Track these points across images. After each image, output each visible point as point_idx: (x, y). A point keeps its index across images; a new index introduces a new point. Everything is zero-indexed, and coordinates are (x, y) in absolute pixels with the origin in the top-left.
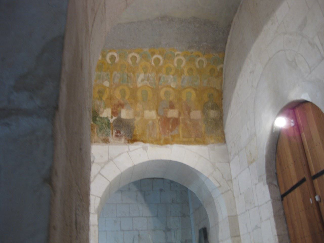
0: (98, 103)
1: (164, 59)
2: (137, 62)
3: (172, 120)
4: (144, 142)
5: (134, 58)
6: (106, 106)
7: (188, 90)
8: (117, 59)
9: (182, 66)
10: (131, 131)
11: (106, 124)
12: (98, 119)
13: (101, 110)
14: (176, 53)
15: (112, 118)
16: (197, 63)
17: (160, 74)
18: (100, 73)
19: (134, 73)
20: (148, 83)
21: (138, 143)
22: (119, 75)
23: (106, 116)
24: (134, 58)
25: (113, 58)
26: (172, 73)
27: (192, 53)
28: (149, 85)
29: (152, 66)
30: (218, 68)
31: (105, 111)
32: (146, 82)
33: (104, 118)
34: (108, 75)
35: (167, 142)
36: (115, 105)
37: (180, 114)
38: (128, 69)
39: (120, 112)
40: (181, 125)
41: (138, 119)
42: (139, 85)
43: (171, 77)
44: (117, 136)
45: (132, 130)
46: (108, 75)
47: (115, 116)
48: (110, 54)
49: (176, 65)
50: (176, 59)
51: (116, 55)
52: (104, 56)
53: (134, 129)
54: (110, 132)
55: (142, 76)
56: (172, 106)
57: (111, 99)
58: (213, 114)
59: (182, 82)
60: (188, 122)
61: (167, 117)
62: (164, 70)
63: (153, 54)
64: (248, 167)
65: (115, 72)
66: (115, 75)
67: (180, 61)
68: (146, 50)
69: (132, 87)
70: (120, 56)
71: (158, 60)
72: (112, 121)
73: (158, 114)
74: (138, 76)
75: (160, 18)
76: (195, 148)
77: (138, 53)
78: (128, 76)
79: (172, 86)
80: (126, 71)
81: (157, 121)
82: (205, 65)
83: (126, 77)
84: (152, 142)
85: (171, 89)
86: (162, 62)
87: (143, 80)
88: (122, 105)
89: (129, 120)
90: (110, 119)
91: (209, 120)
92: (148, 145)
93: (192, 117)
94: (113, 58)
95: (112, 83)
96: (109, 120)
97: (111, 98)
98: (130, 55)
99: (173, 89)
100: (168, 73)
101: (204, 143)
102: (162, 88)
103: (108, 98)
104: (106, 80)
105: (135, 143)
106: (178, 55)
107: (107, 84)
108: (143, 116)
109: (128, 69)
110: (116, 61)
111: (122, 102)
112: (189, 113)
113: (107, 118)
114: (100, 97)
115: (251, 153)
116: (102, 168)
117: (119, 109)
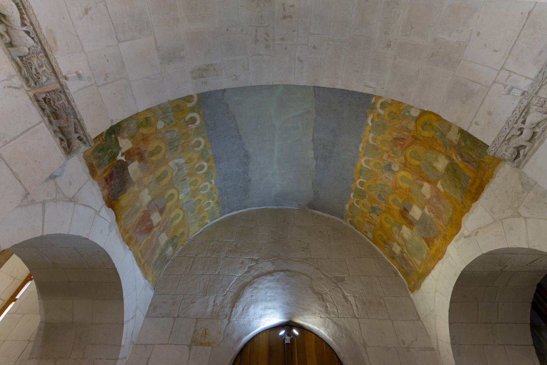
0: (132, 125)
2: (196, 149)
4: (117, 220)
5: (199, 144)
6: (132, 137)
7: (181, 213)
8: (193, 126)
9: (202, 192)
10: (119, 192)
11: (111, 153)
12: (113, 136)
13: (125, 135)
14: (213, 181)
15: (123, 154)
16: (207, 202)
17: (188, 178)
19: (182, 151)
21: (113, 212)
22: (175, 136)
23: (121, 145)
24: (199, 144)
27: (215, 193)
28: (174, 173)
29: (195, 165)
31: (126, 139)
33: (118, 145)
35: (128, 241)
36: (139, 148)
37: (158, 224)
39: (133, 161)
40: (150, 237)
41: (136, 188)
42: (171, 164)
43: (189, 189)
44: (106, 180)
45: (121, 192)
46: (172, 122)
47: (125, 158)
49: (201, 187)
50: (207, 183)
51: (198, 122)
52: (192, 110)
53: (123, 193)
54: (105, 165)
55: (181, 161)
56: (161, 212)
57: (143, 139)
59: (187, 202)
62: (194, 179)
63: (208, 161)
64: (190, 347)
65: (176, 129)
66: (175, 131)
67: (206, 187)
68: (210, 152)
69: (167, 157)
70: (198, 127)
71: (202, 167)
72: (120, 157)
73: (149, 205)
74: (180, 158)
76: (138, 272)
77: (205, 146)
79: (180, 196)
80: (182, 141)
82: (206, 209)
84: (120, 227)
85: (177, 196)
86: (201, 172)
87: (177, 164)
88: (141, 158)
90: (120, 154)
92: (116, 226)
93: (159, 238)
94: (193, 120)
95: (163, 132)
96: (117, 154)
97: (145, 139)
98: (200, 139)
99: (178, 198)
100: (191, 184)
101: (146, 276)
102: (175, 188)
103: (143, 135)
104: (165, 122)
105: (111, 209)
106: (211, 183)
107: (160, 125)
108: (140, 192)
110: (190, 126)
111: (146, 155)
112: (162, 232)
113: (120, 148)
114: (141, 123)
115: (206, 332)
116: (55, 200)
117: (137, 157)
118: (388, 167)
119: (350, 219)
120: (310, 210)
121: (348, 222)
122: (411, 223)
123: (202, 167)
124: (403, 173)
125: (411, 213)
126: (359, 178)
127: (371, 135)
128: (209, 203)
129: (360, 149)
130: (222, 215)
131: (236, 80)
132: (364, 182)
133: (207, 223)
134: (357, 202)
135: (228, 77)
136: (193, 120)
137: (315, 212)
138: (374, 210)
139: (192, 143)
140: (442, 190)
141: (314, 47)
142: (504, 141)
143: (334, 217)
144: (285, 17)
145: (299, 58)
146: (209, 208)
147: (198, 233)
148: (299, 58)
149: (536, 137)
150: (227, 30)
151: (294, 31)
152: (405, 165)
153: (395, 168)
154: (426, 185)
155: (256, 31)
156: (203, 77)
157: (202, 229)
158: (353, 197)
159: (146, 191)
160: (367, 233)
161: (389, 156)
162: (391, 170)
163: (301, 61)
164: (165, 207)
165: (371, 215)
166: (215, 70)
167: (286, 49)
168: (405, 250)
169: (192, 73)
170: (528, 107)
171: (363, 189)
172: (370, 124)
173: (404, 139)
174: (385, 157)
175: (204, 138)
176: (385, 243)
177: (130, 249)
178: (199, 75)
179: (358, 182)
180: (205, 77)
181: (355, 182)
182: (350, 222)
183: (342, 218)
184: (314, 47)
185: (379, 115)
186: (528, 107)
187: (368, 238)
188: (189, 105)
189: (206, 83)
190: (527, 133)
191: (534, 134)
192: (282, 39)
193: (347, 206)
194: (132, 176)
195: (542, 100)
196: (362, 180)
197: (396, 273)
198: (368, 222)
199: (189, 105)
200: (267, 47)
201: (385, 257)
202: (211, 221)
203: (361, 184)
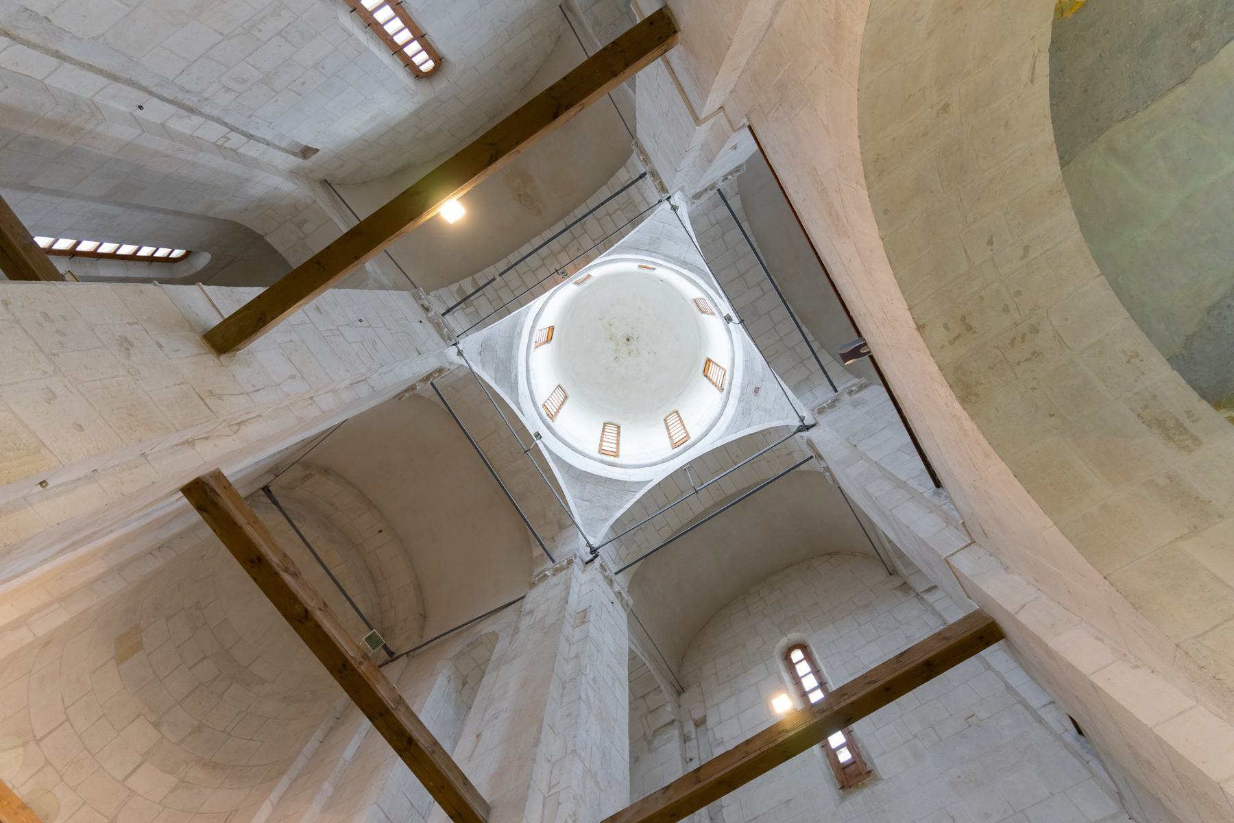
131: (1137, 355)
135: (1143, 373)
141: (990, 242)
144: (969, 328)
145: (1023, 258)
148: (1025, 256)
150: (1051, 415)
151: (982, 298)
155: (1019, 363)
156: (1179, 424)
163: (1027, 249)
166: (1146, 407)
167: (1018, 293)
169: (1189, 450)
178: (1181, 434)
180: (1177, 420)
184: (990, 242)
189: (1189, 413)
192: (1006, 309)
200: (1035, 330)
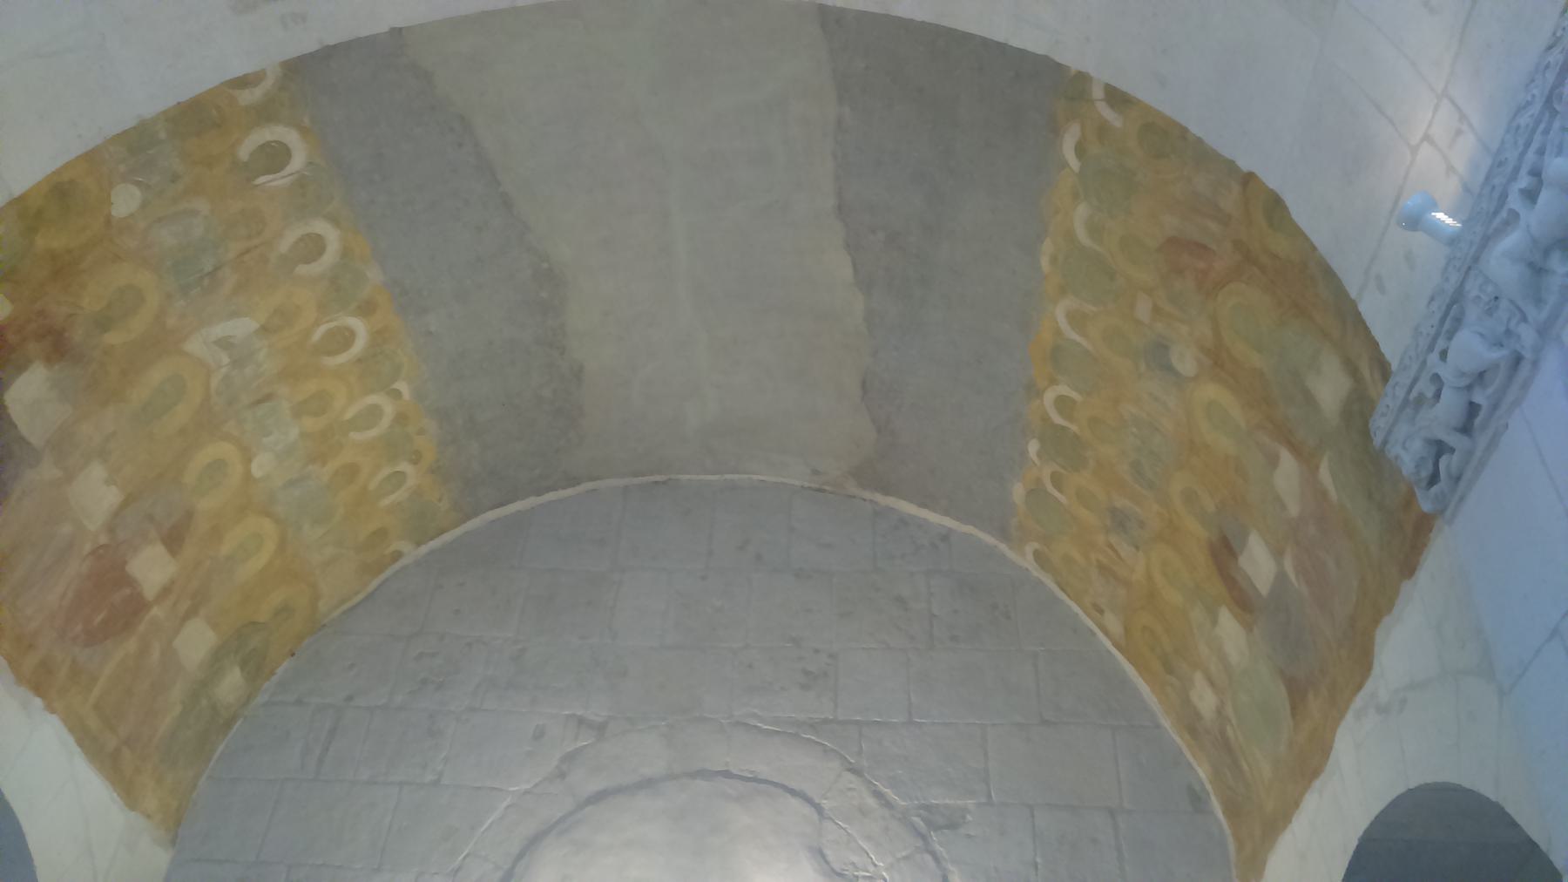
1: (359, 360)
2: (302, 269)
3: (127, 591)
5: (313, 247)
7: (268, 526)
9: (355, 436)
14: (402, 386)
16: (386, 471)
18: (163, 135)
20: (224, 370)
24: (313, 247)
25: (275, 156)
26: (309, 423)
27: (421, 432)
28: (215, 382)
30: (395, 546)
32: (226, 360)
34: (175, 178)
37: (166, 591)
38: (248, 251)
39: (21, 368)
40: (132, 645)
41: (47, 471)
42: (195, 346)
43: (294, 433)
46: (175, 178)
48: (291, 137)
49: (349, 415)
51: (298, 161)
52: (265, 113)
55: (241, 328)
58: (232, 682)
60: (156, 654)
61: (125, 563)
62: (312, 386)
65: (202, 205)
67: (374, 413)
68: (374, 275)
71: (347, 338)
74: (234, 314)
75: (545, 265)
76: (94, 787)
77: (346, 253)
78: (217, 269)
81: (88, 547)
82: (386, 502)
83: (208, 268)
86: (341, 359)
87: (225, 344)
88: (57, 346)
89: (22, 440)
91: (204, 702)
97: (64, 269)
98: (320, 227)
99: (248, 477)
100: (298, 412)
101: (128, 792)
106: (397, 394)
107: (125, 201)
109: (248, 251)
110: (261, 180)
118: (1158, 355)
119: (1036, 545)
120: (867, 495)
121: (1030, 557)
122: (1243, 601)
123: (344, 339)
124: (1211, 391)
125: (1243, 561)
126: (1053, 381)
127: (1082, 211)
128: (400, 477)
129: (1045, 263)
130: (468, 518)
132: (1074, 402)
133: (398, 556)
134: (1057, 480)
136: (275, 156)
137: (890, 501)
138: (1119, 521)
139: (285, 245)
140: (1333, 493)
142: (1406, 402)
143: (969, 529)
146: (399, 495)
147: (360, 597)
149: (1477, 421)
152: (1218, 361)
153: (1186, 361)
154: (1287, 461)
157: (375, 583)
158: (1039, 455)
159: (97, 471)
160: (1101, 612)
161: (1157, 311)
162: (1169, 369)
164: (189, 515)
165: (1113, 539)
168: (1229, 710)
170: (1458, 297)
171: (1074, 428)
172: (1074, 163)
173: (1205, 247)
174: (1143, 309)
175: (334, 220)
176: (1170, 670)
177: (51, 709)
179: (1049, 396)
181: (1039, 394)
182: (1037, 555)
183: (1003, 533)
185: (1103, 130)
186: (1458, 297)
187: (1106, 633)
188: (247, 97)
190: (1450, 405)
191: (1473, 409)
193: (1018, 492)
194: (24, 429)
195: (1490, 289)
196: (1063, 389)
197: (1197, 800)
198: (1102, 568)
199: (247, 97)
201: (1166, 723)
202: (418, 544)
203: (1063, 404)
